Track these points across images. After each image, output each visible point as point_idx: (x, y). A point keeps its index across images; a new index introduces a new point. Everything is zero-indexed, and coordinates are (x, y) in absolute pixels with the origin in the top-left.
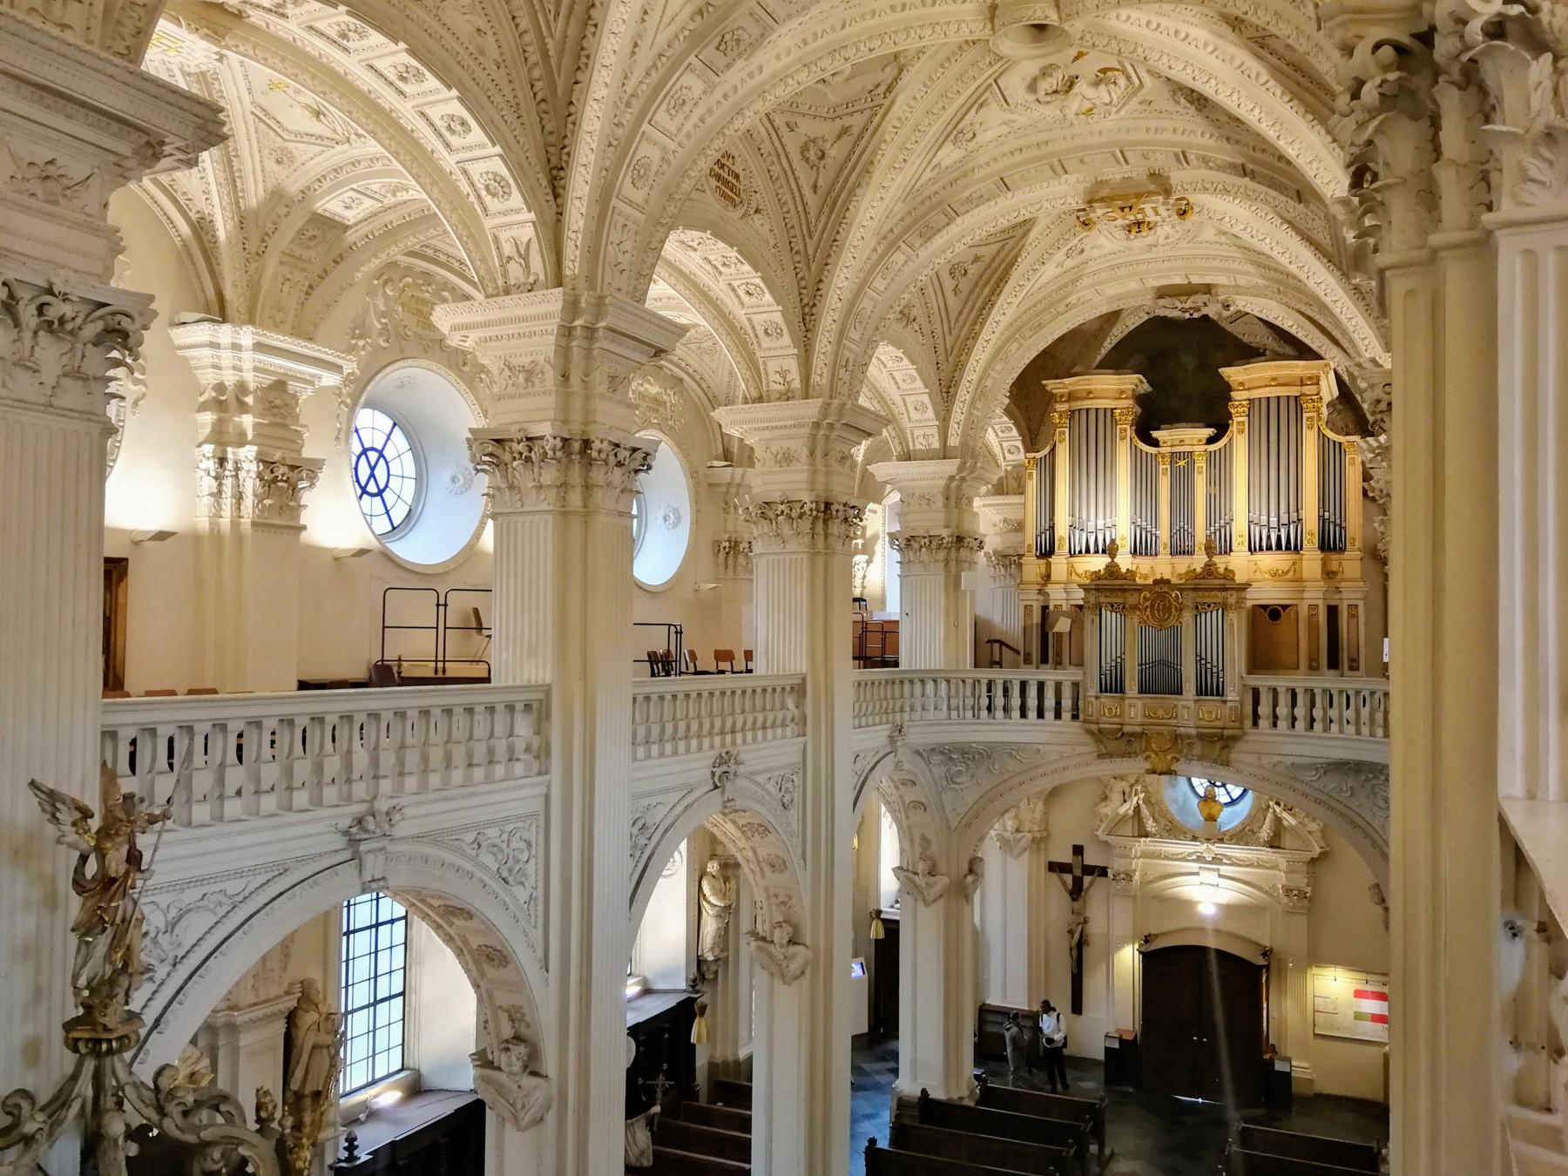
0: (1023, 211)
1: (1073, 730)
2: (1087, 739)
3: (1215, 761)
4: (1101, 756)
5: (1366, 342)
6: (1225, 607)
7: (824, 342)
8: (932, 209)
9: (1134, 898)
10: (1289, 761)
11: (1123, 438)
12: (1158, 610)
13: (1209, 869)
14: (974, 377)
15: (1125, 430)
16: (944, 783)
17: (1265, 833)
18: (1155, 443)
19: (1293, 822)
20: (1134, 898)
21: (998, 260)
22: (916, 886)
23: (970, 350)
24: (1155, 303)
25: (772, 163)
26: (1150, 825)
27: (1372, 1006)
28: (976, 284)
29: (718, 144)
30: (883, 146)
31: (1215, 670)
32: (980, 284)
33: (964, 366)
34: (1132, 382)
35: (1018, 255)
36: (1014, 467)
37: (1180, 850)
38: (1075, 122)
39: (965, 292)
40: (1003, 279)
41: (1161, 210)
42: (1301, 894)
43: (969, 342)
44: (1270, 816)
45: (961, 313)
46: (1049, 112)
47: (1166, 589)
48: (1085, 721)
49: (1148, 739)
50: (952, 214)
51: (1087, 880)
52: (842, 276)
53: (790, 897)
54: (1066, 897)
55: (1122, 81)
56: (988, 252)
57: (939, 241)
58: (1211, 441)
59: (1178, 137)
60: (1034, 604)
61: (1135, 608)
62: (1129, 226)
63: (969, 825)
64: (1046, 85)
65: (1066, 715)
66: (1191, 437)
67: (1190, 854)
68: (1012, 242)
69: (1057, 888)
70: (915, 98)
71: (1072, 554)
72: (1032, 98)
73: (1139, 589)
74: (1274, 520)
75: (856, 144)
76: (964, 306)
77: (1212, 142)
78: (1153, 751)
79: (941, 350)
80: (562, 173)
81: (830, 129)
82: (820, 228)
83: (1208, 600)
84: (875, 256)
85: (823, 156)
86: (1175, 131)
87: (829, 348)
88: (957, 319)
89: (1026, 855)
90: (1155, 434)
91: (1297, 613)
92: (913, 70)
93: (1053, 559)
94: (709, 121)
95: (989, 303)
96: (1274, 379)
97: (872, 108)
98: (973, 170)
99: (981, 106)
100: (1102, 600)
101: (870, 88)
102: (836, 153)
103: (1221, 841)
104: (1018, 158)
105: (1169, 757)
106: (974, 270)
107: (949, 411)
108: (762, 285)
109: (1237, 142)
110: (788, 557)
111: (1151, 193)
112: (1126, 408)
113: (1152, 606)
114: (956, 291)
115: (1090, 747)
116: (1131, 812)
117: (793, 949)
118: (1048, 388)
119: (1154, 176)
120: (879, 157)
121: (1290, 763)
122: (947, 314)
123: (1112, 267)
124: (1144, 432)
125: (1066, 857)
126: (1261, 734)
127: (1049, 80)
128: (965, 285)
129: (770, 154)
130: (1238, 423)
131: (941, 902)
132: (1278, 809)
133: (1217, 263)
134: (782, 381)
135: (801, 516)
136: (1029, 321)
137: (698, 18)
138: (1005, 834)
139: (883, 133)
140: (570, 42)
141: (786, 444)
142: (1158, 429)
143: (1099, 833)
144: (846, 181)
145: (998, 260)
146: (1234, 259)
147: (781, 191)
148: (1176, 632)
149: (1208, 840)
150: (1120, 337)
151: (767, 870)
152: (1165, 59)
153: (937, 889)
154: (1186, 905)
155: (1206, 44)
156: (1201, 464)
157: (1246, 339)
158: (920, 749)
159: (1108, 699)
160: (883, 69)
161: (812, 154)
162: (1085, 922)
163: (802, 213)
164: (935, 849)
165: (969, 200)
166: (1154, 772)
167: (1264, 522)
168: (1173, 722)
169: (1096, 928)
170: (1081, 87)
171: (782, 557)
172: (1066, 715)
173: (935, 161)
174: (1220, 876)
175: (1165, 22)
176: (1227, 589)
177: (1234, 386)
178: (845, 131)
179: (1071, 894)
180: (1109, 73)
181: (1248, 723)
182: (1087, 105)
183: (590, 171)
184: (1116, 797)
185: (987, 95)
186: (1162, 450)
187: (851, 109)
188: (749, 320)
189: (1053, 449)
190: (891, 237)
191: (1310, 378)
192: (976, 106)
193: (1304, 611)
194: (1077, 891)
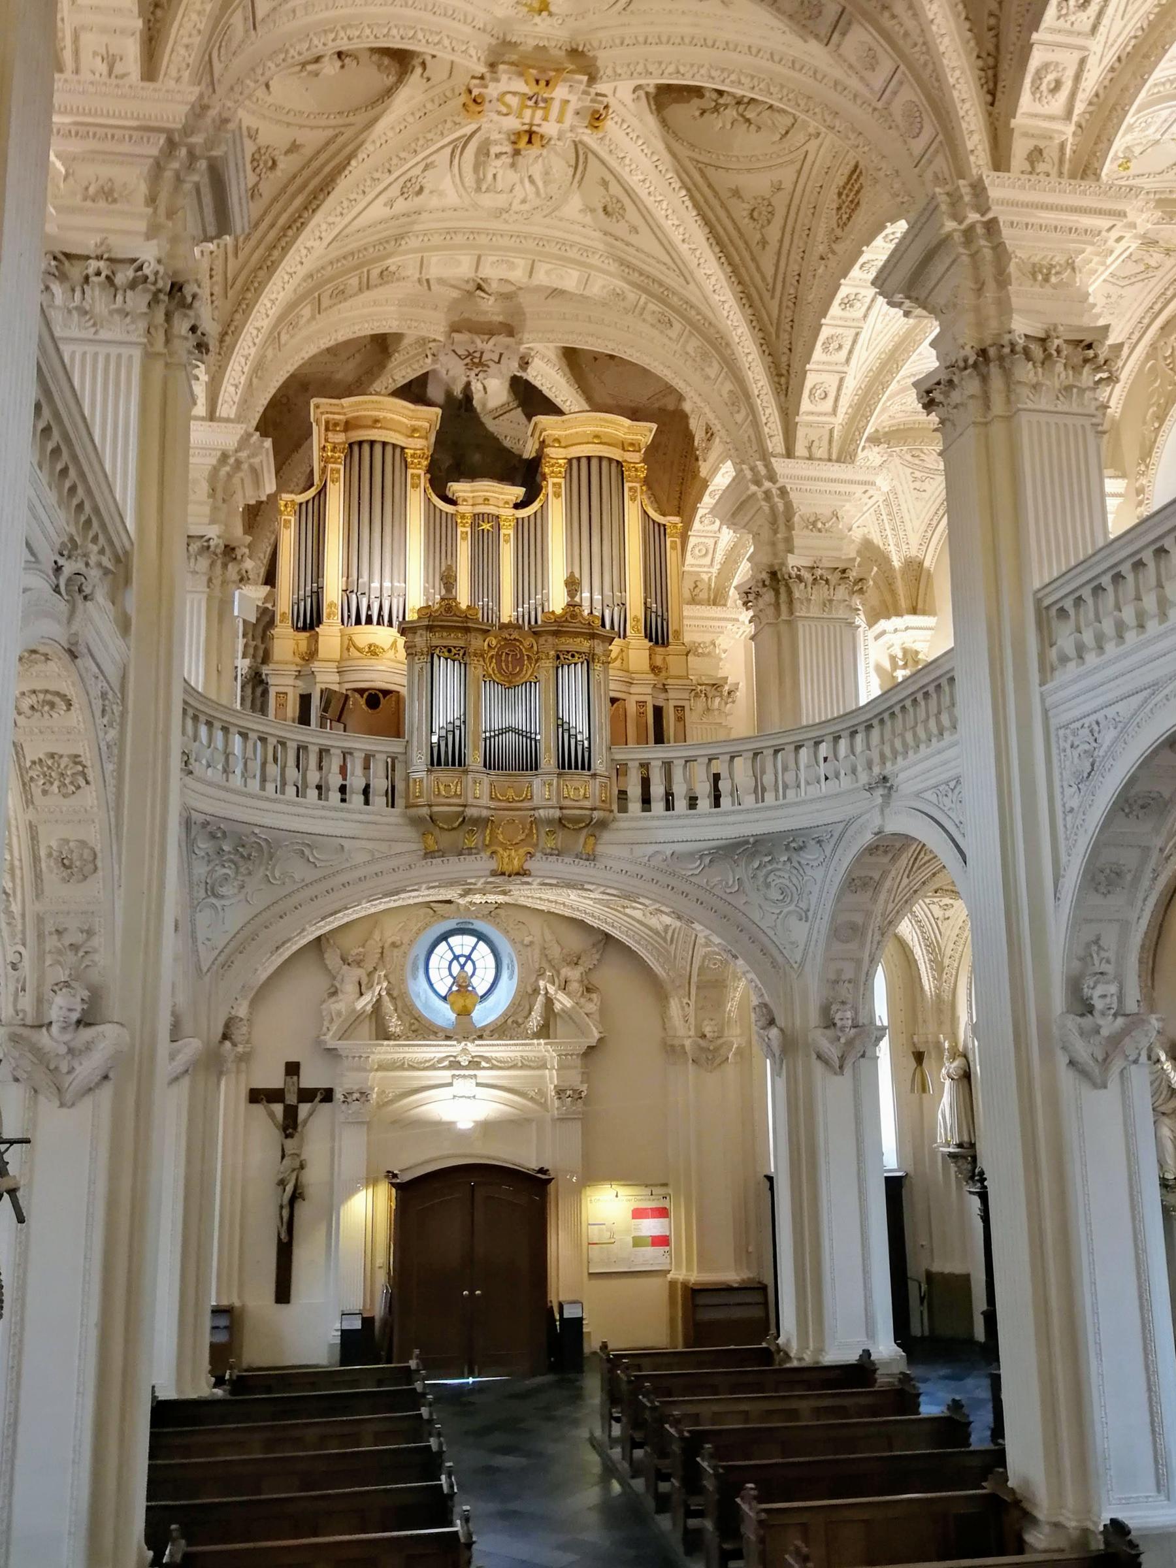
1: (392, 820)
4: (429, 854)
6: (590, 659)
9: (368, 1124)
10: (668, 850)
13: (464, 1076)
15: (419, 476)
16: (202, 894)
17: (535, 1020)
20: (368, 1124)
21: (323, 157)
26: (394, 1024)
27: (651, 1227)
28: (284, 190)
32: (292, 189)
33: (250, 307)
37: (428, 1056)
40: (326, 187)
42: (578, 1096)
43: (261, 273)
44: (541, 999)
47: (515, 635)
51: (304, 1109)
53: (90, 933)
54: (276, 1134)
56: (311, 139)
58: (517, 506)
60: (290, 690)
61: (481, 655)
62: (518, 134)
63: (227, 965)
65: (379, 801)
67: (441, 1060)
69: (265, 1120)
74: (597, 597)
79: (218, 278)
87: (197, 40)
90: (458, 488)
95: (297, 223)
96: (596, 436)
103: (480, 1037)
105: (522, 851)
106: (286, 165)
110: (102, 350)
112: (419, 446)
115: (410, 842)
116: (369, 1008)
117: (86, 1034)
119: (574, 53)
121: (669, 853)
124: (438, 483)
125: (274, 1079)
126: (633, 819)
128: (268, 189)
130: (554, 484)
131: (186, 1081)
132: (552, 990)
133: (573, 254)
134: (103, 68)
135: (133, 285)
141: (106, 171)
143: (327, 1038)
145: (323, 157)
151: (52, 874)
154: (441, 1129)
156: (508, 531)
157: (507, 443)
158: (195, 816)
162: (302, 1167)
169: (314, 1176)
171: (90, 349)
174: (478, 1085)
179: (285, 1129)
181: (615, 807)
184: (350, 988)
186: (462, 509)
191: (632, 444)
193: (632, 708)
194: (290, 1125)
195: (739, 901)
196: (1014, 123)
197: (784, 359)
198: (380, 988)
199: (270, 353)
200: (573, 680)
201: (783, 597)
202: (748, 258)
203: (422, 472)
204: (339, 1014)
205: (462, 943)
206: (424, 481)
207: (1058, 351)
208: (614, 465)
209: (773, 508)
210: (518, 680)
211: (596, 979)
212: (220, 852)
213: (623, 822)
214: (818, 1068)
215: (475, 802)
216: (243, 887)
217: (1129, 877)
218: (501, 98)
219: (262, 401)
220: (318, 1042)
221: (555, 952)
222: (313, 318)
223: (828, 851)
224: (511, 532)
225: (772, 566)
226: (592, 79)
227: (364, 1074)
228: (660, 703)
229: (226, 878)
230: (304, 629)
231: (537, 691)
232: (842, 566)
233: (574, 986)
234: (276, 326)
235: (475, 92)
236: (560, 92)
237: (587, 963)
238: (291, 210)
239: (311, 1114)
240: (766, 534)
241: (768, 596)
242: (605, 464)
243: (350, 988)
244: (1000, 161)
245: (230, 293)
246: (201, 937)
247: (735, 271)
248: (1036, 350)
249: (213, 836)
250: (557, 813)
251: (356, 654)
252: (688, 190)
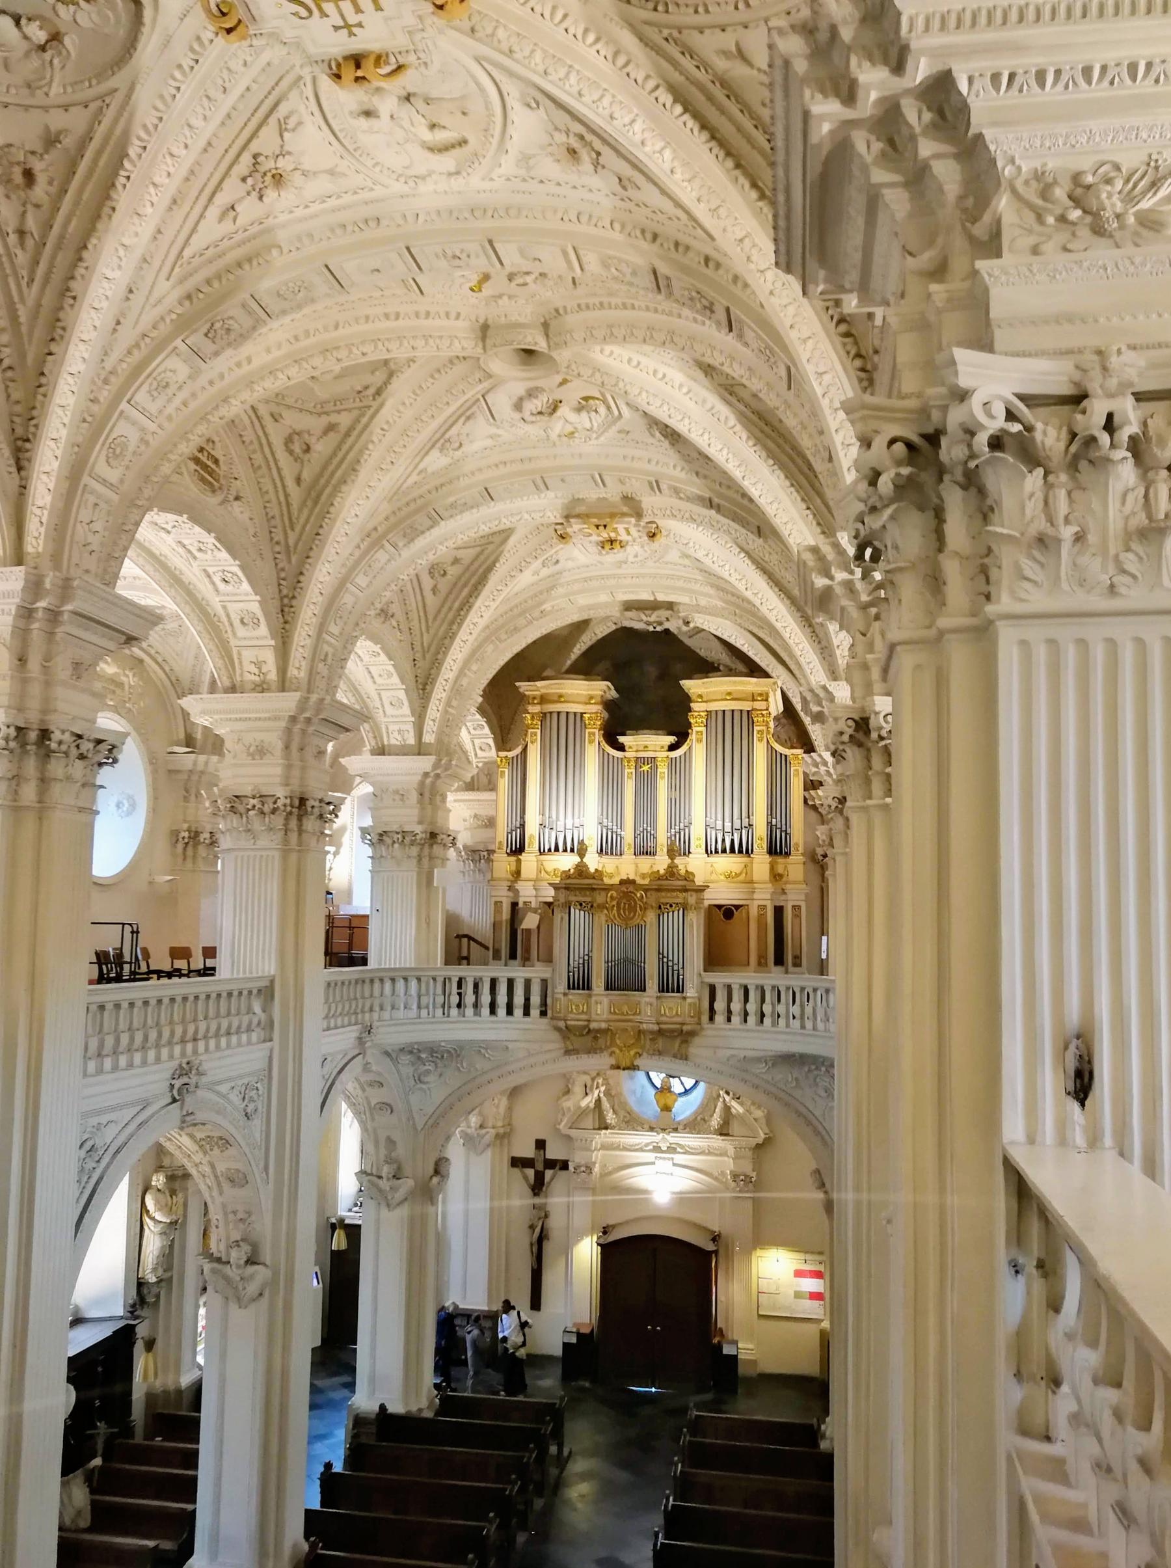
0: (504, 520)
1: (543, 1027)
2: (556, 1035)
3: (675, 1056)
4: (568, 1052)
5: (811, 666)
7: (303, 636)
8: (418, 511)
10: (742, 1054)
11: (591, 742)
12: (624, 910)
13: (664, 1158)
14: (451, 676)
15: (594, 734)
16: (413, 1082)
17: (716, 1121)
18: (621, 748)
19: (741, 1110)
21: (476, 565)
22: (380, 1190)
23: (448, 649)
24: (622, 614)
25: (254, 452)
26: (610, 1118)
29: (202, 429)
30: (370, 446)
31: (676, 968)
33: (441, 664)
34: (601, 688)
36: (485, 764)
37: (637, 1141)
38: (558, 443)
39: (443, 594)
41: (633, 531)
42: (748, 1180)
44: (720, 1105)
45: (439, 611)
46: (533, 431)
47: (631, 889)
48: (552, 1018)
49: (613, 1034)
50: (436, 518)
51: (549, 1173)
52: (324, 570)
55: (602, 410)
56: (467, 555)
57: (421, 542)
58: (673, 747)
59: (652, 467)
60: (504, 900)
61: (602, 907)
62: (602, 542)
63: (436, 1125)
64: (531, 406)
65: (535, 1012)
66: (655, 743)
67: (647, 1145)
68: (491, 547)
69: (520, 1180)
70: (404, 404)
71: (541, 852)
72: (517, 416)
73: (607, 889)
75: (342, 442)
76: (442, 606)
77: (683, 475)
78: (618, 1046)
79: (418, 648)
80: (27, 445)
81: (316, 424)
82: (302, 520)
83: (671, 901)
84: (357, 553)
85: (308, 449)
86: (649, 461)
87: (308, 642)
88: (435, 618)
89: (489, 1153)
90: (621, 739)
91: (748, 913)
92: (402, 377)
93: (523, 857)
94: (193, 405)
95: (466, 605)
96: (729, 694)
97: (360, 408)
98: (458, 478)
99: (468, 418)
100: (573, 898)
101: (359, 388)
102: (322, 448)
103: (676, 1130)
104: (503, 470)
105: (632, 1053)
106: (453, 571)
107: (424, 707)
108: (240, 574)
109: (705, 477)
110: (259, 853)
111: (624, 515)
112: (594, 713)
113: (618, 904)
114: (434, 590)
115: (555, 1043)
116: (592, 1105)
117: (251, 1269)
118: (521, 690)
119: (627, 499)
120: (366, 457)
122: (425, 612)
123: (585, 580)
124: (611, 736)
125: (528, 1152)
127: (535, 401)
128: (444, 585)
129: (251, 442)
131: (406, 1205)
132: (727, 1098)
133: (680, 584)
135: (274, 811)
137: (187, 303)
138: (469, 1131)
139: (371, 433)
140: (44, 312)
142: (624, 734)
143: (561, 1127)
144: (333, 474)
145: (476, 565)
146: (696, 581)
147: (261, 480)
148: (640, 928)
149: (664, 1130)
150: (589, 643)
151: (226, 1186)
152: (644, 395)
153: (400, 1195)
155: (681, 386)
156: (663, 769)
157: (702, 653)
159: (576, 996)
160: (373, 373)
161: (297, 448)
162: (546, 1216)
163: (284, 504)
164: (401, 1151)
165: (453, 506)
166: (618, 1068)
167: (719, 826)
168: (638, 1018)
169: (555, 1223)
170: (564, 411)
171: (252, 853)
172: (535, 1012)
173: (421, 466)
174: (674, 1164)
175: (644, 361)
176: (686, 890)
177: (694, 697)
178: (331, 428)
179: (533, 1190)
180: (591, 402)
181: (705, 1017)
182: (569, 429)
183: (61, 446)
184: (578, 1089)
185: (475, 408)
186: (627, 754)
187: (339, 407)
188: (224, 607)
189: (525, 750)
190: (374, 535)
191: (760, 695)
192: (463, 419)
193: (754, 912)
194: (538, 1186)
195: (798, 1094)
199: (465, 682)
203: (596, 731)
204: (569, 1109)
206: (598, 736)
213: (709, 1029)
215: (597, 1018)
216: (441, 1075)
227: (589, 1153)
238: (461, 598)
239: (552, 1179)
245: (428, 656)
250: (656, 1028)
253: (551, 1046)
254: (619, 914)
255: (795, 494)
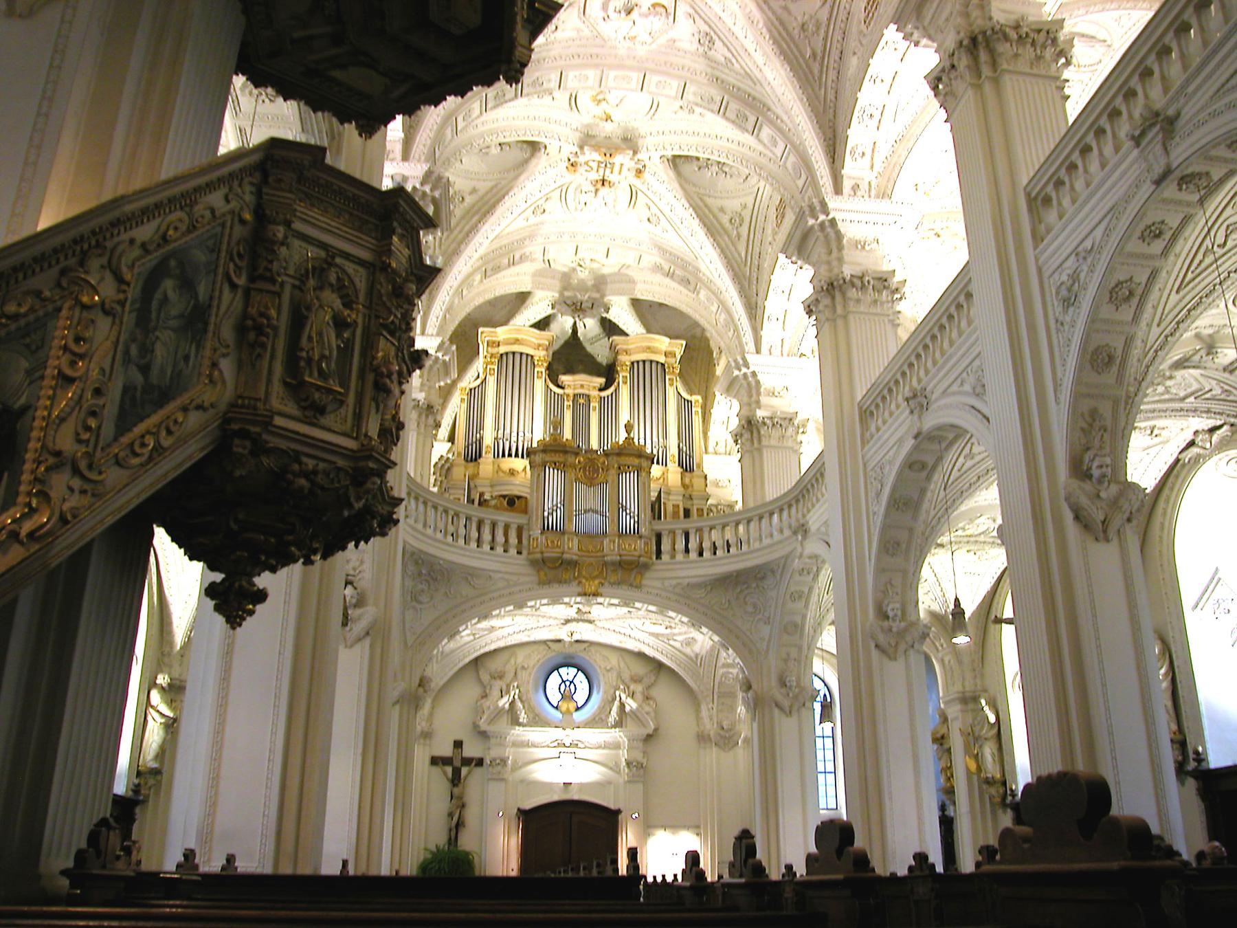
2: (529, 570)
3: (631, 585)
6: (639, 470)
10: (687, 581)
14: (456, 284)
21: (489, 195)
26: (523, 717)
35: (507, 193)
42: (640, 766)
44: (617, 703)
51: (464, 771)
54: (447, 785)
56: (483, 187)
61: (574, 466)
71: (497, 456)
72: (602, 14)
78: (584, 577)
83: (629, 463)
87: (429, 142)
90: (564, 379)
115: (528, 576)
116: (507, 706)
119: (625, 139)
124: (553, 375)
125: (446, 750)
126: (664, 564)
136: (493, 259)
145: (489, 195)
154: (549, 786)
156: (595, 404)
162: (463, 806)
170: (634, 15)
180: (657, 9)
181: (654, 557)
184: (496, 693)
186: (567, 391)
191: (670, 353)
194: (456, 780)
196: (843, 172)
197: (754, 299)
198: (514, 692)
199: (456, 301)
200: (629, 482)
201: (755, 434)
202: (730, 245)
205: (568, 673)
207: (868, 282)
208: (659, 366)
209: (749, 384)
210: (596, 481)
211: (654, 693)
212: (420, 574)
213: (658, 565)
214: (776, 711)
216: (432, 598)
217: (904, 546)
218: (586, 163)
219: (451, 328)
220: (475, 726)
221: (626, 675)
222: (481, 281)
223: (778, 577)
224: (597, 405)
225: (748, 417)
226: (635, 153)
228: (688, 506)
229: (423, 591)
230: (471, 460)
231: (608, 489)
232: (789, 416)
233: (639, 696)
234: (460, 286)
235: (572, 160)
236: (618, 159)
237: (647, 681)
239: (469, 773)
240: (745, 399)
241: (747, 435)
242: (654, 365)
243: (496, 693)
244: (838, 190)
246: (407, 626)
247: (722, 251)
248: (858, 283)
249: (417, 563)
251: (500, 473)
252: (694, 209)
253: (527, 579)
254: (585, 474)
255: (796, 82)
